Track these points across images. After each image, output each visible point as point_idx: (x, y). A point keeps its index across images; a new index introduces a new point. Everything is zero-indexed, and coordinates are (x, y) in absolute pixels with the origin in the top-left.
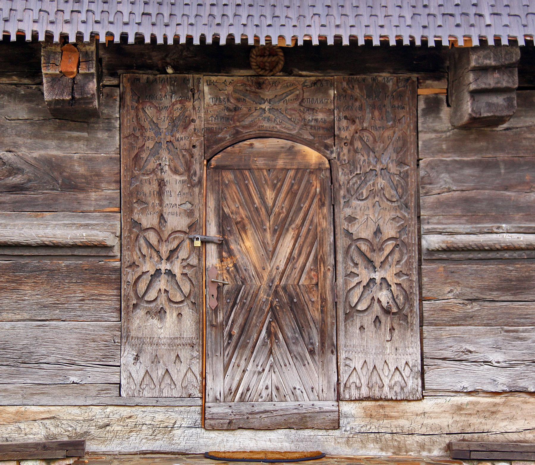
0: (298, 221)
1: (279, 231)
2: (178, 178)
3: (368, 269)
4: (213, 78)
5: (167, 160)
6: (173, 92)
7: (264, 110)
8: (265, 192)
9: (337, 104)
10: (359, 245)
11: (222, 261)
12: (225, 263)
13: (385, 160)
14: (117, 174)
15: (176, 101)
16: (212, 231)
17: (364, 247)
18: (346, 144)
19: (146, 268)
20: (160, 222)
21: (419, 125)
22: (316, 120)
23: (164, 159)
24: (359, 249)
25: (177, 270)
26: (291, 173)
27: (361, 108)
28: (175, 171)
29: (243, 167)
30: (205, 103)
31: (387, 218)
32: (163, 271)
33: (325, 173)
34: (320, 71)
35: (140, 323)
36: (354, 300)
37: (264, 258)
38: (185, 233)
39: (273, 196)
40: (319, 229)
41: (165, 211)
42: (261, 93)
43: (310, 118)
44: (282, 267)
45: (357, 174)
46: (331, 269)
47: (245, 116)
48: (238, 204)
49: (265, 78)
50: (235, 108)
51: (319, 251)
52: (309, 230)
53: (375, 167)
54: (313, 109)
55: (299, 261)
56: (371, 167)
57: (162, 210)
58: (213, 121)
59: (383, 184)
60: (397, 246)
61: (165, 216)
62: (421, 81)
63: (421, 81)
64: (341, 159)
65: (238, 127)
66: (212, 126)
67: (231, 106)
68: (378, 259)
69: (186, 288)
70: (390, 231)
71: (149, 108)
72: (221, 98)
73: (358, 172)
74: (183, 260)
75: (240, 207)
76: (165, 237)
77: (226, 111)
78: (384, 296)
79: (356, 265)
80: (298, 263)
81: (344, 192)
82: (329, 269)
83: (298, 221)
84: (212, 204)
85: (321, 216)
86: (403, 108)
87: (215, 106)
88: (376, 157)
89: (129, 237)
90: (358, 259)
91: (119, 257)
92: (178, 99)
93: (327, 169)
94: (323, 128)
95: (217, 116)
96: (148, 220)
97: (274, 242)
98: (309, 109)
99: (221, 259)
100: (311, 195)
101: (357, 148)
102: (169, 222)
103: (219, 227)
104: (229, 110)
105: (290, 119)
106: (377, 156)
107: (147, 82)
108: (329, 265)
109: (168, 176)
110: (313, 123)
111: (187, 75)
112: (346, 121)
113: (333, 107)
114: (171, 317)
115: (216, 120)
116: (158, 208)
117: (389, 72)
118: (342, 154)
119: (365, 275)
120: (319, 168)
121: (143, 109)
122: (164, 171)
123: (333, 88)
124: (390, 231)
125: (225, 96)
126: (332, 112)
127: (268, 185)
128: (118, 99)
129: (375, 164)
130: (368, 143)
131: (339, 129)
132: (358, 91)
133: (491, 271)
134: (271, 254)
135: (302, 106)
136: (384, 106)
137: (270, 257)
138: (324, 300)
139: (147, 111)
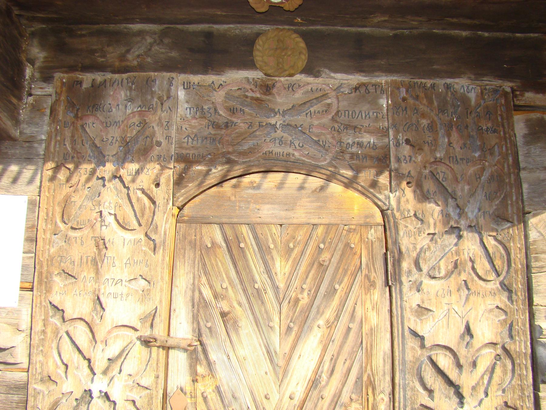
0: (329, 313)
2: (129, 236)
3: (450, 398)
4: (196, 79)
5: (113, 206)
6: (131, 100)
7: (274, 126)
8: (274, 264)
9: (393, 119)
10: (434, 358)
11: (195, 381)
12: (200, 387)
13: (472, 212)
14: (33, 226)
15: (133, 113)
17: (444, 361)
18: (410, 185)
20: (95, 309)
21: (521, 158)
22: (360, 145)
23: (107, 204)
24: (434, 364)
26: (320, 230)
27: (432, 127)
29: (235, 220)
30: (179, 115)
31: (482, 309)
32: (96, 394)
33: (376, 231)
34: (362, 74)
38: (136, 330)
39: (287, 269)
40: (366, 329)
41: (102, 291)
42: (269, 100)
43: (350, 141)
44: (299, 395)
45: (429, 234)
46: (386, 399)
47: (243, 137)
48: (227, 282)
49: (277, 79)
50: (227, 123)
51: (366, 368)
52: (349, 329)
53: (457, 222)
54: (355, 128)
55: (330, 384)
56: (452, 223)
58: (190, 144)
59: (472, 251)
60: (498, 357)
62: (518, 93)
63: (518, 93)
64: (402, 208)
65: (229, 153)
66: (188, 151)
67: (221, 121)
68: (466, 381)
71: (91, 125)
72: (206, 107)
73: (432, 231)
74: (130, 375)
75: (230, 289)
77: (211, 127)
79: (431, 392)
80: (328, 388)
81: (410, 264)
82: (383, 399)
83: (329, 313)
84: (183, 281)
85: (368, 305)
86: (495, 131)
87: (194, 121)
88: (458, 206)
89: (44, 332)
91: (26, 366)
92: (135, 110)
93: (378, 225)
94: (371, 157)
95: (196, 135)
97: (287, 349)
98: (347, 127)
100: (352, 268)
101: (428, 191)
103: (193, 323)
104: (216, 126)
105: (317, 142)
106: (461, 203)
107: (92, 86)
108: (382, 392)
110: (354, 149)
111: (152, 74)
112: (408, 147)
113: (386, 124)
115: (195, 143)
116: (91, 285)
117: (469, 78)
118: (403, 200)
121: (82, 126)
122: (107, 223)
123: (385, 96)
125: (211, 106)
126: (384, 133)
127: (278, 252)
128: (48, 111)
129: (457, 218)
130: (444, 183)
131: (398, 160)
132: (425, 101)
134: (281, 370)
135: (337, 122)
136: (467, 127)
137: (280, 378)
139: (87, 129)
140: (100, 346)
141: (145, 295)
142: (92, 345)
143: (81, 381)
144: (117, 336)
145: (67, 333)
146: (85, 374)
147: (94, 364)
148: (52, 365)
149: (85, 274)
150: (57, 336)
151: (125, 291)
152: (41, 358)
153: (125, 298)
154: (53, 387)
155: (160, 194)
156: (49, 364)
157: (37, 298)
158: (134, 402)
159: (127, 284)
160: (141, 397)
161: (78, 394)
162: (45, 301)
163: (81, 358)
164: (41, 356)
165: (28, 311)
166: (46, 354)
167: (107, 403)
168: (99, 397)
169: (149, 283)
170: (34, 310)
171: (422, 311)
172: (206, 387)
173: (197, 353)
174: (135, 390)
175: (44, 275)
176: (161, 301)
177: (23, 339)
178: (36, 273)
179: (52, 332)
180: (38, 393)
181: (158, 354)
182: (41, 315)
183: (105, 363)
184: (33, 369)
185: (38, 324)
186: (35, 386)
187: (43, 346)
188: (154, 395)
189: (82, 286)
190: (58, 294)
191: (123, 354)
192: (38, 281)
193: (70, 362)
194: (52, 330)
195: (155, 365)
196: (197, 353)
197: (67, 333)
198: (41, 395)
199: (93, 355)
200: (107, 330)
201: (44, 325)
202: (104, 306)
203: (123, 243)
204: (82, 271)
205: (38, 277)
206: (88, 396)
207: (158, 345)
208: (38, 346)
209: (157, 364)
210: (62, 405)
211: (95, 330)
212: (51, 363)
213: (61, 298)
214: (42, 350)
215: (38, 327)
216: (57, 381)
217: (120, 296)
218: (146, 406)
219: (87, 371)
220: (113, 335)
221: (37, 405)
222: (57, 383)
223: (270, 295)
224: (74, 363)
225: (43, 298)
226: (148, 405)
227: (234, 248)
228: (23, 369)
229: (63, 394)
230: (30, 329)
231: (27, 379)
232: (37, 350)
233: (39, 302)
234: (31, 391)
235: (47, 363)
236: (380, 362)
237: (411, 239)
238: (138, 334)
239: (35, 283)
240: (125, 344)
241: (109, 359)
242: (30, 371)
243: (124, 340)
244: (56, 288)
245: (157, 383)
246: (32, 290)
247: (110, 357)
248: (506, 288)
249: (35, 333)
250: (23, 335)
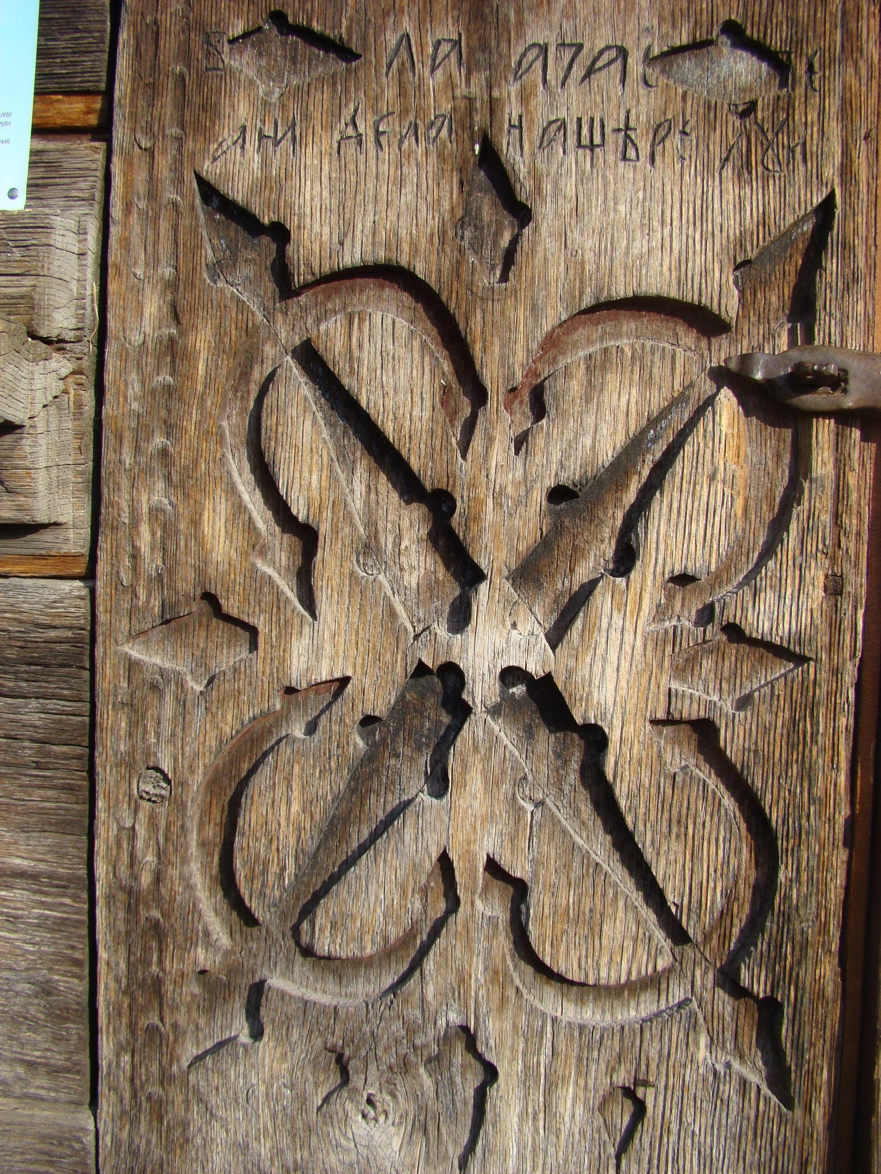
19: (317, 652)
25: (616, 672)
32: (482, 689)
41: (512, 110)
57: (493, 106)
61: (518, 159)
69: (702, 863)
74: (683, 580)
76: (503, 359)
91: (75, 541)
96: (356, 187)
102: (547, 216)
116: (439, 86)
140: (501, 423)
141: (758, 137)
142: (452, 416)
143: (393, 614)
144: (597, 367)
145: (310, 358)
146: (412, 580)
147: (474, 518)
148: (226, 530)
149: (407, 25)
150: (245, 375)
151: (644, 107)
152: (156, 494)
153: (644, 147)
154: (229, 656)
156: (207, 529)
157: (129, 163)
158: (704, 733)
159: (653, 74)
160: (744, 703)
161: (376, 694)
162: (178, 182)
163: (389, 495)
164: (160, 485)
165: (81, 232)
166: (189, 471)
167: (545, 740)
168: (495, 711)
169: (779, 65)
170: (114, 230)
174: (707, 664)
175: (170, 44)
176: (846, 170)
177: (56, 387)
178: (124, 36)
179: (218, 348)
180: (154, 687)
181: (841, 464)
182: (157, 260)
183: (530, 521)
184: (116, 556)
185: (140, 306)
186: (133, 651)
187: (170, 429)
188: (821, 693)
189: (391, 93)
190: (252, 143)
191: (652, 461)
192: (137, 76)
193: (327, 514)
194: (220, 333)
195: (826, 518)
197: (310, 358)
198: (169, 698)
199: (464, 467)
200: (547, 327)
201: (176, 317)
202: (524, 190)
204: (385, 14)
205: (138, 54)
206: (431, 701)
207: (849, 402)
208: (142, 433)
209: (837, 516)
210: (285, 750)
211: (475, 327)
212: (220, 524)
213: (265, 164)
214: (164, 453)
215: (143, 319)
216: (260, 622)
217: (614, 141)
218: (779, 752)
219: (418, 563)
220: (575, 358)
221: (148, 754)
222: (253, 631)
224: (349, 517)
225: (164, 164)
226: (791, 746)
228: (65, 558)
229: (290, 691)
230: (91, 336)
231: (84, 608)
232: (137, 450)
233: (141, 187)
234: (109, 675)
235: (196, 522)
238: (723, 351)
239: (121, 89)
240: (657, 400)
241: (559, 494)
242: (102, 568)
243: (647, 382)
244: (242, 110)
245: (835, 626)
246: (102, 131)
247: (571, 474)
249: (124, 356)
250: (61, 364)
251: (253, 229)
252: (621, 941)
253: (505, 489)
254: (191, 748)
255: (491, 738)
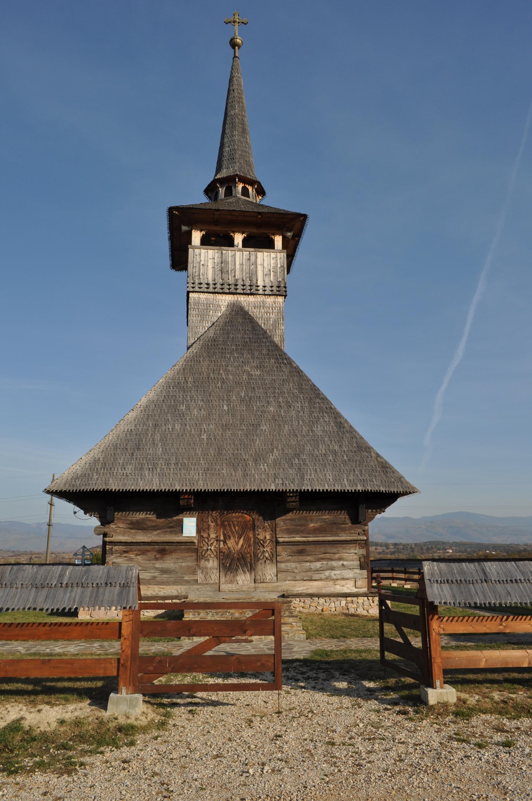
1: (240, 538)
16: (222, 538)
17: (261, 542)
25: (212, 548)
28: (212, 522)
35: (203, 563)
36: (259, 556)
37: (235, 545)
68: (265, 545)
69: (215, 554)
70: (268, 537)
78: (267, 555)
84: (222, 531)
90: (261, 545)
96: (205, 535)
99: (224, 545)
109: (210, 523)
114: (211, 562)
119: (262, 549)
120: (250, 521)
124: (268, 537)
133: (295, 548)
134: (237, 544)
138: (251, 556)
141: (216, 533)
148: (202, 545)
155: (218, 517)
171: (258, 534)
172: (226, 547)
173: (225, 542)
196: (225, 542)
203: (212, 525)
223: (235, 532)
227: (229, 525)
236: (252, 542)
237: (257, 523)
248: (272, 530)
251: (202, 536)
252: (213, 556)
253: (209, 543)
254: (201, 551)
255: (209, 551)
